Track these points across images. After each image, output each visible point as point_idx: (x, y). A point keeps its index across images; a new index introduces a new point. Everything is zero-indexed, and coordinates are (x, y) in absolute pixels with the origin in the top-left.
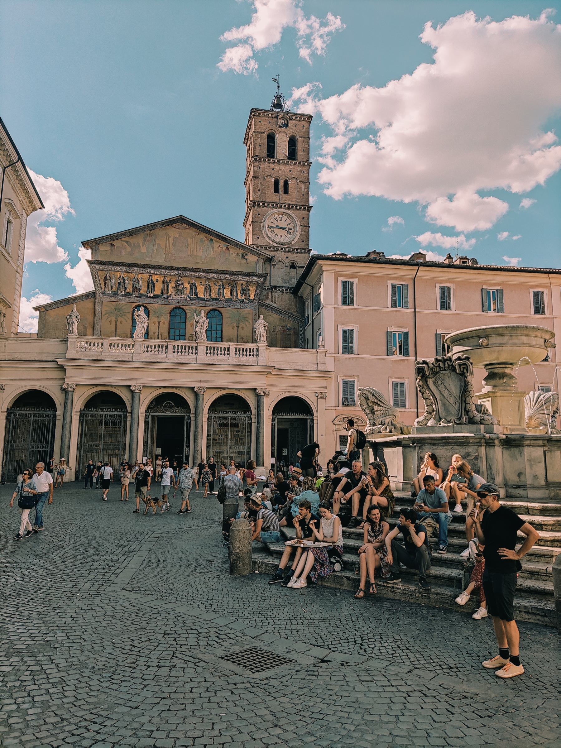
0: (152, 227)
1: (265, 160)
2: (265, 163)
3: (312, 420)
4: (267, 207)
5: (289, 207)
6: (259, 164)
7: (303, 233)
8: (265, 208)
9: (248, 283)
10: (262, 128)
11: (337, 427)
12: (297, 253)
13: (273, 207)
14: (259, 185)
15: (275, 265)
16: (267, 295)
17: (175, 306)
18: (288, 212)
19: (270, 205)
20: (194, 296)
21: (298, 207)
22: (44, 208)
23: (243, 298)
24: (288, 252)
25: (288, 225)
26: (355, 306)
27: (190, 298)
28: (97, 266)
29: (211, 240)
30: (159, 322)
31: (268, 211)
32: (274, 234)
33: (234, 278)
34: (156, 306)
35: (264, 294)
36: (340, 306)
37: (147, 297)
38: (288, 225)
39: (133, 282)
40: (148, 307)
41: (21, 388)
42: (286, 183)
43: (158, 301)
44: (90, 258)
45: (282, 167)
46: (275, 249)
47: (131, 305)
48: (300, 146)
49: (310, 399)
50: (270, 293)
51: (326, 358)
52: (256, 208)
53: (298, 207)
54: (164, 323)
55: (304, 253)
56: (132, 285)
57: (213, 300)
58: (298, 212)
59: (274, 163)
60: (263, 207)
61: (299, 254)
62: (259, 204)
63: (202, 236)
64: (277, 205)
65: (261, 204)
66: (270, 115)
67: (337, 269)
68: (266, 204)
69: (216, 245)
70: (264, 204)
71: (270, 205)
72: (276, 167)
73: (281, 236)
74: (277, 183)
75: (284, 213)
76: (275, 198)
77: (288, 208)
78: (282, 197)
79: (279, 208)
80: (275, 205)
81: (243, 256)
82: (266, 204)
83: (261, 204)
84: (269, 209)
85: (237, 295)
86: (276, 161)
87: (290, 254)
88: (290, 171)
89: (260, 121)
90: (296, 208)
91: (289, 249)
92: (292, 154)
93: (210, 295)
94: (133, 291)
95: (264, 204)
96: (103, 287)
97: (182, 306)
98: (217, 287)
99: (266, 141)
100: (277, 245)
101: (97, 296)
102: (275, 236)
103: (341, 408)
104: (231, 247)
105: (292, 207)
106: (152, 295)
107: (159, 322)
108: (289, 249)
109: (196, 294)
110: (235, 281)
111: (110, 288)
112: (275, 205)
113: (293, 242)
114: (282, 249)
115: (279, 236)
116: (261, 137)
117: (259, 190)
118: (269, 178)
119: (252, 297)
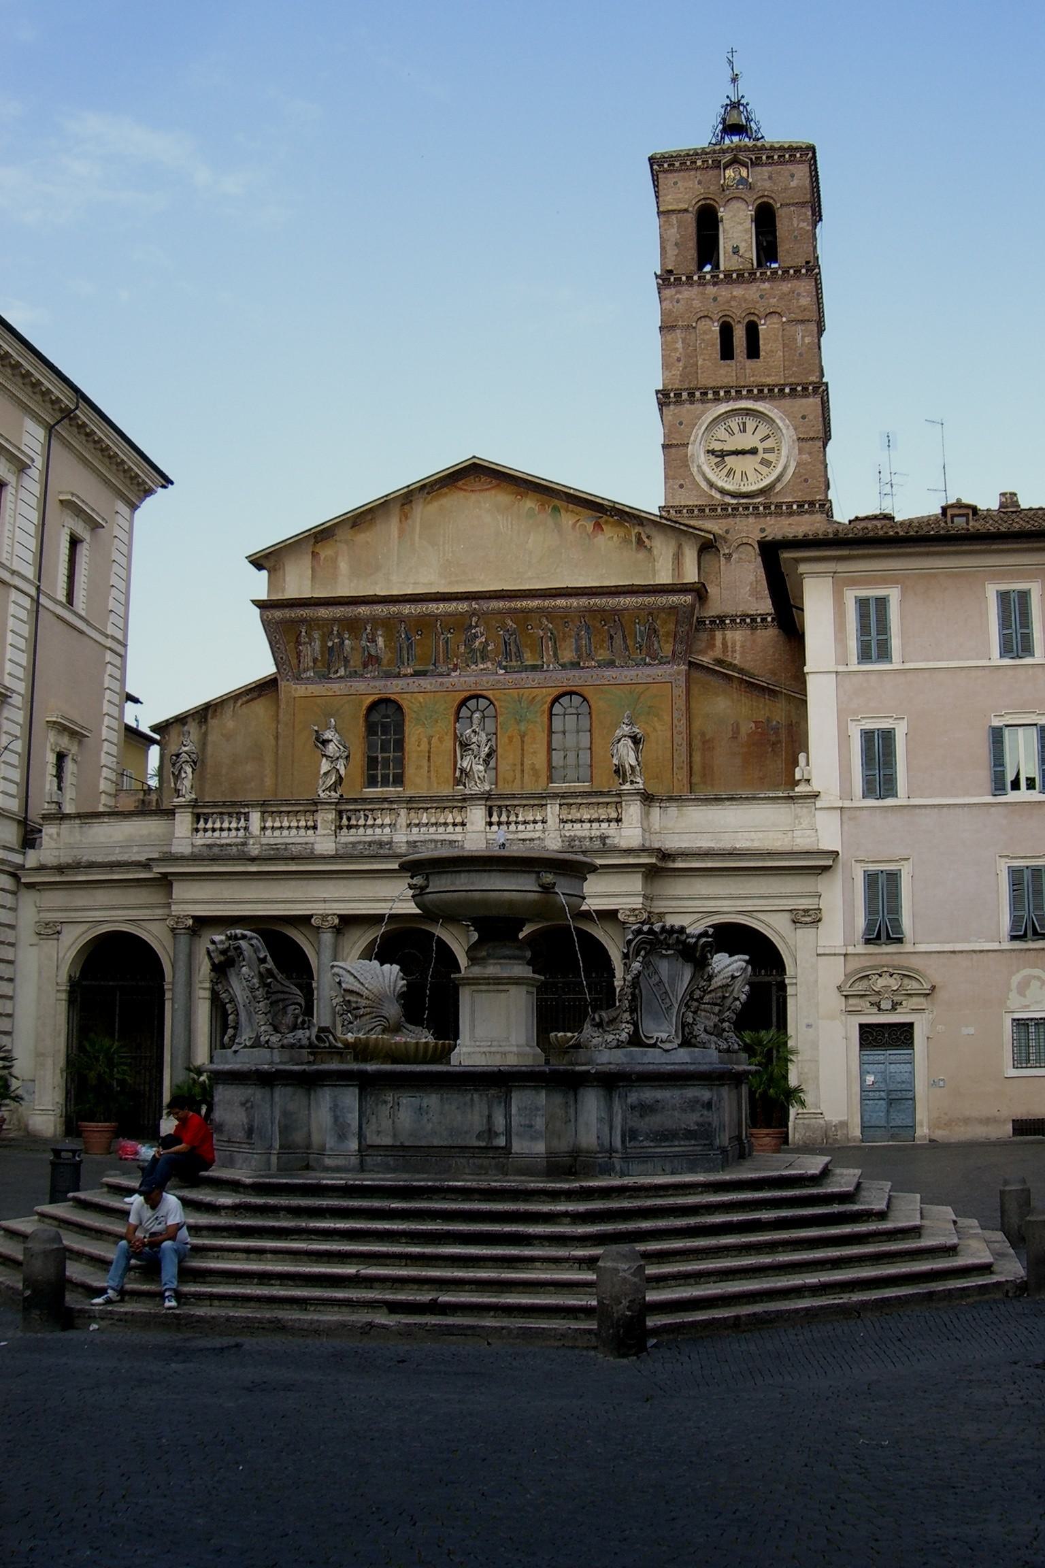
0: (407, 499)
1: (689, 278)
2: (691, 285)
3: (782, 987)
4: (702, 401)
5: (761, 391)
6: (677, 292)
7: (805, 457)
8: (699, 406)
9: (652, 612)
10: (679, 201)
11: (852, 1001)
12: (791, 514)
13: (717, 399)
14: (679, 345)
15: (730, 555)
16: (713, 638)
17: (467, 694)
18: (760, 406)
19: (710, 396)
20: (514, 663)
21: (787, 390)
22: (172, 483)
23: (644, 652)
24: (765, 515)
25: (762, 440)
26: (896, 664)
27: (505, 668)
28: (278, 614)
29: (556, 509)
30: (430, 738)
31: (703, 413)
32: (725, 471)
33: (611, 602)
34: (421, 697)
35: (704, 636)
36: (855, 666)
37: (398, 676)
38: (762, 440)
39: (363, 643)
40: (401, 702)
41: (89, 929)
42: (752, 331)
43: (426, 683)
44: (263, 596)
45: (738, 291)
46: (727, 511)
47: (361, 701)
48: (789, 223)
49: (776, 928)
50: (719, 635)
51: (817, 813)
52: (672, 407)
53: (787, 390)
54: (441, 740)
55: (811, 513)
56: (361, 650)
57: (563, 666)
58: (787, 402)
59: (715, 284)
60: (692, 403)
61: (796, 518)
62: (678, 395)
63: (530, 504)
64: (727, 392)
65: (685, 395)
66: (699, 163)
67: (841, 567)
68: (698, 394)
69: (567, 520)
70: (691, 395)
71: (710, 396)
72: (724, 292)
73: (744, 475)
74: (726, 331)
75: (748, 412)
76: (726, 373)
77: (760, 397)
78: (741, 370)
79: (735, 399)
80: (722, 393)
81: (640, 542)
82: (698, 394)
83: (685, 395)
84: (709, 405)
85: (627, 649)
86: (721, 276)
87: (770, 520)
88: (761, 297)
89: (675, 183)
90: (782, 390)
91: (766, 507)
92: (767, 249)
93: (555, 655)
94: (365, 665)
95: (691, 395)
96: (294, 661)
97: (484, 693)
98: (573, 633)
99: (692, 229)
100: (734, 501)
101: (282, 684)
102: (728, 475)
103: (861, 949)
104: (606, 522)
105: (771, 390)
106: (410, 671)
107: (430, 738)
108: (766, 507)
109: (519, 656)
110: (616, 612)
111: (311, 664)
112: (722, 393)
113: (779, 487)
114: (747, 508)
115: (738, 475)
116: (680, 222)
117: (679, 360)
118: (703, 325)
119: (667, 649)
